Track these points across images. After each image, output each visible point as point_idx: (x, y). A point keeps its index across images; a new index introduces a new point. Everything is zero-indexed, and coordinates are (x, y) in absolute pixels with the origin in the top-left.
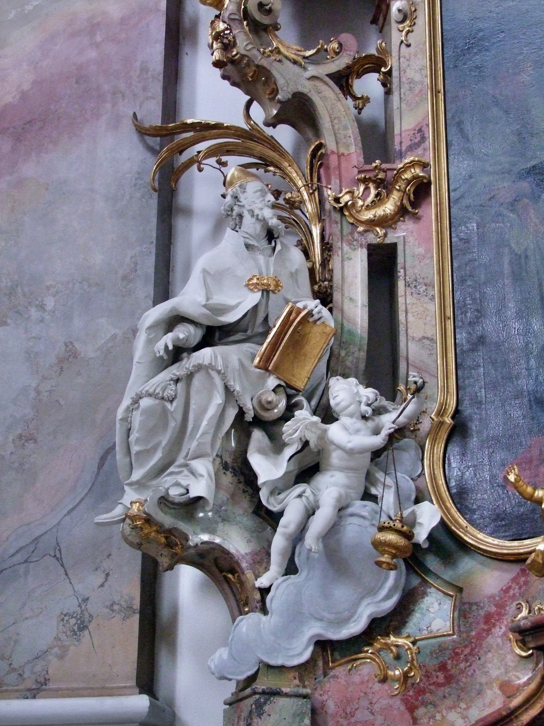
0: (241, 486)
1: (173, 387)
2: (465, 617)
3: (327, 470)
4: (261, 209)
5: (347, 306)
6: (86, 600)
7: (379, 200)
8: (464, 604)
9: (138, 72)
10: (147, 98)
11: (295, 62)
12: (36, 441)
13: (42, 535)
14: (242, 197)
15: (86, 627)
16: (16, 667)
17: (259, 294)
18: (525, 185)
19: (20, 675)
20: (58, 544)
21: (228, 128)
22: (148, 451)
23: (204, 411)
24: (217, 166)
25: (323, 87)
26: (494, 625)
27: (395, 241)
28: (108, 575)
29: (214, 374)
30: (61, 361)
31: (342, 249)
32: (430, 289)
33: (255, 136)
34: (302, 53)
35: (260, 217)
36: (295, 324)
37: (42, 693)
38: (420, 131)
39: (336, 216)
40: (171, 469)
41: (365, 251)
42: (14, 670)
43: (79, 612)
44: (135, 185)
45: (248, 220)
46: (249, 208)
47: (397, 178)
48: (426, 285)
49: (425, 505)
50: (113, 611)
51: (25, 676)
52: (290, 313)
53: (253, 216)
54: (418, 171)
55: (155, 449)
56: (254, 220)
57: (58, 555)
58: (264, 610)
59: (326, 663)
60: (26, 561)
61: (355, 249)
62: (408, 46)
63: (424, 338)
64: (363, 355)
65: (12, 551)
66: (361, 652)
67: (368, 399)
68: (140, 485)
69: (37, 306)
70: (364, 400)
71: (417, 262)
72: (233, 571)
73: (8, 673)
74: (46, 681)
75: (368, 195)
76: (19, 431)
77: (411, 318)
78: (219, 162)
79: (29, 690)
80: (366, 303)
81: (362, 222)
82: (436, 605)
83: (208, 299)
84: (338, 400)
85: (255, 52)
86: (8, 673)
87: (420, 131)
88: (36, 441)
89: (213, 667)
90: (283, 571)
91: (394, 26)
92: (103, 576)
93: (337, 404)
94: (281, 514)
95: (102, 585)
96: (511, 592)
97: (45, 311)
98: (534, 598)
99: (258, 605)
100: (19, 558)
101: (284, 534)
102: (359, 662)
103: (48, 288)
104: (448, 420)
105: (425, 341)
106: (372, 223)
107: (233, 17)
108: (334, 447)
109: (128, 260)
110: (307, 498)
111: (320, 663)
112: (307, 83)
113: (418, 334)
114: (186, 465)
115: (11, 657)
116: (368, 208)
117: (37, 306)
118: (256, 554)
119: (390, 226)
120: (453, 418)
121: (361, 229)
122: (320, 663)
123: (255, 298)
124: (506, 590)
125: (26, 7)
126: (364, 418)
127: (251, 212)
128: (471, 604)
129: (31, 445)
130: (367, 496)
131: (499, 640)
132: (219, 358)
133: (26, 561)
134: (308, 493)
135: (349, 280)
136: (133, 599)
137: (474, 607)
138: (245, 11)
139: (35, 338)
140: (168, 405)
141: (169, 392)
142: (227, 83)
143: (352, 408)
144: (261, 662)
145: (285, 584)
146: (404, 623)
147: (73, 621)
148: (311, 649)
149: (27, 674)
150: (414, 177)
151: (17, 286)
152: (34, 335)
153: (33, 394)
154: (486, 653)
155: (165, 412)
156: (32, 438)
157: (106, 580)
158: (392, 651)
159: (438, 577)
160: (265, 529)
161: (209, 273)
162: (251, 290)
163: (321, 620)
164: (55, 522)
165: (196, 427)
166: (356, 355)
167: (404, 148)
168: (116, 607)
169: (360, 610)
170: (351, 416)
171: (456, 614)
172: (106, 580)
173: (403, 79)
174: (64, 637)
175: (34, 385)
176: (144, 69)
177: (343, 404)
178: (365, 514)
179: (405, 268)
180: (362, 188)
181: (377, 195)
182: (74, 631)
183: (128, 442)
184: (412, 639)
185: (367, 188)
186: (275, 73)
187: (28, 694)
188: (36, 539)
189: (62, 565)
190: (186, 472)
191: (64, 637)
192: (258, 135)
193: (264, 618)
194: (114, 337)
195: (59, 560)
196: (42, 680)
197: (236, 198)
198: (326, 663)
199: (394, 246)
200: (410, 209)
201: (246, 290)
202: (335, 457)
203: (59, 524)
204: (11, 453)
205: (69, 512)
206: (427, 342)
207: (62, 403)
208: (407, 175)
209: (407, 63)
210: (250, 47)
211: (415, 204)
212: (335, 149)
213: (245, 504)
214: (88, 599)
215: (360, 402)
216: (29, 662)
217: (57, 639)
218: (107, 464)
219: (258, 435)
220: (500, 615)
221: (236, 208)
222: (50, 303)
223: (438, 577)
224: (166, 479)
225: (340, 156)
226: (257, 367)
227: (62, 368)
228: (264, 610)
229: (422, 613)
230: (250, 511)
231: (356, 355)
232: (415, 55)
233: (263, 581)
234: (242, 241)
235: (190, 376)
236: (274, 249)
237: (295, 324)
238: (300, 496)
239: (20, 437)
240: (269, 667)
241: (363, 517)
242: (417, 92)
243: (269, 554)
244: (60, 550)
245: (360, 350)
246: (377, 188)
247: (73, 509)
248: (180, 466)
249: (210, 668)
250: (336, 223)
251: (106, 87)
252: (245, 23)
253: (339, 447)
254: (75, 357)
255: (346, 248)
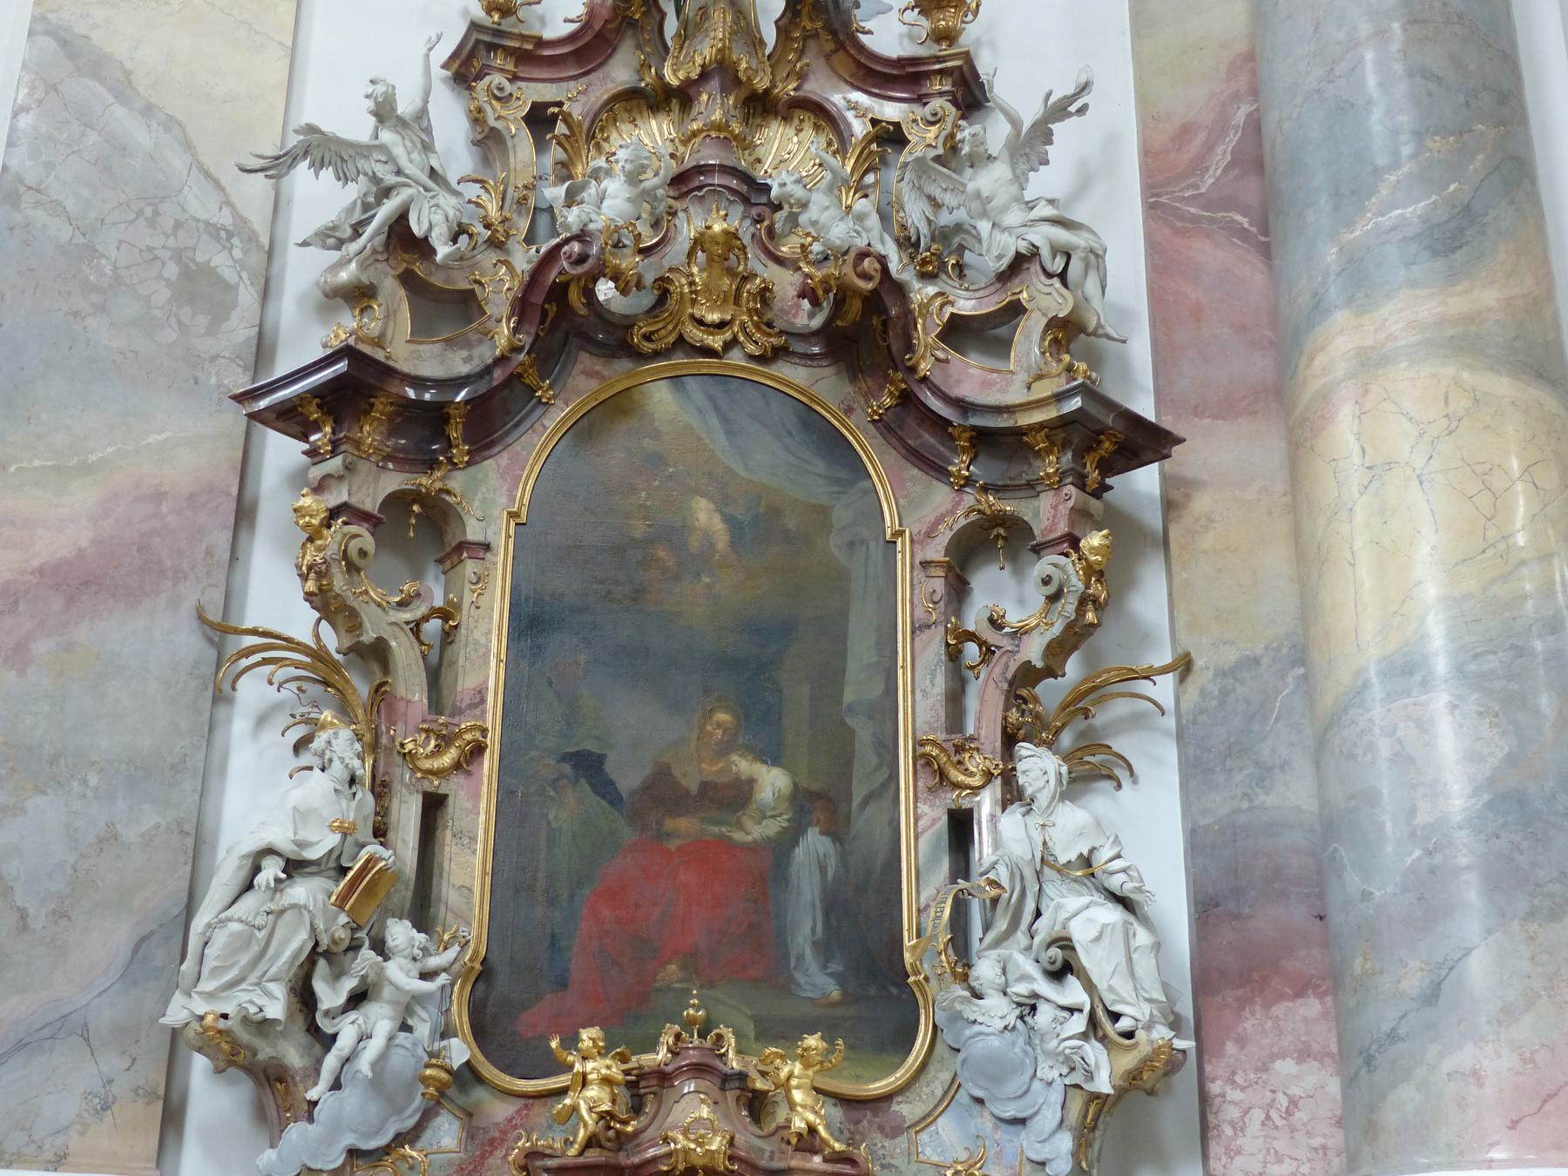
0: (299, 1006)
1: (265, 918)
2: (472, 1139)
3: (376, 1000)
4: (352, 759)
5: (399, 846)
6: (111, 1082)
7: (438, 751)
8: (473, 1127)
9: (203, 555)
10: (210, 585)
11: (379, 605)
12: (69, 919)
13: (71, 1013)
14: (334, 743)
15: (109, 1107)
16: (36, 1139)
17: (340, 835)
18: (567, 768)
19: (40, 1147)
20: (86, 1024)
21: (298, 643)
22: (225, 967)
23: (287, 941)
24: (297, 692)
25: (401, 634)
26: (496, 1148)
27: (447, 792)
28: (134, 1059)
29: (305, 913)
30: (101, 840)
31: (401, 791)
32: (473, 842)
33: (322, 657)
34: (386, 598)
35: (350, 766)
36: (373, 872)
37: (64, 1167)
38: (480, 692)
39: (399, 760)
40: (243, 986)
41: (420, 798)
42: (34, 1141)
43: (103, 1092)
44: (191, 674)
45: (337, 764)
46: (340, 755)
47: (459, 735)
48: (470, 838)
49: (455, 1042)
50: (137, 1095)
51: (44, 1148)
52: (368, 861)
53: (342, 763)
54: (478, 735)
55: (231, 966)
56: (342, 767)
57: (85, 1035)
58: (311, 1119)
59: (352, 1168)
60: (52, 1038)
61: (411, 793)
62: (478, 608)
63: (463, 886)
64: (409, 894)
65: (38, 1026)
66: (381, 1160)
67: (421, 943)
68: (210, 996)
69: (79, 780)
70: (417, 944)
71: (464, 816)
72: (281, 1080)
73: (28, 1144)
74: (65, 1156)
75: (429, 744)
76: (53, 906)
77: (453, 866)
78: (299, 689)
79: (50, 1162)
80: (417, 847)
81: (420, 770)
82: (447, 1125)
83: (295, 834)
84: (397, 942)
85: (350, 594)
86: (28, 1144)
87: (480, 692)
88: (69, 919)
89: (261, 1166)
90: (328, 1086)
91: (468, 586)
92: (131, 1060)
93: (396, 946)
94: (334, 1037)
95: (128, 1069)
96: (514, 1122)
97: (88, 786)
98: (532, 1130)
99: (306, 1115)
100: (46, 1033)
101: (337, 1056)
102: (379, 1169)
103: (93, 763)
104: (478, 967)
105: (464, 890)
106: (431, 772)
107: (334, 556)
108: (387, 982)
109: (177, 749)
110: (359, 1026)
111: (348, 1168)
112: (387, 627)
113: (459, 883)
114: (258, 984)
115: (31, 1128)
116: (427, 757)
117: (79, 780)
118: (307, 1069)
119: (444, 777)
120: (482, 964)
121: (419, 775)
122: (348, 1168)
123: (333, 840)
124: (510, 1121)
125: (90, 456)
126: (415, 959)
127: (342, 760)
128: (478, 1128)
129: (64, 922)
130: (405, 1027)
131: (499, 1161)
132: (311, 899)
133: (52, 1038)
134: (361, 1021)
135: (402, 822)
136: (158, 1085)
137: (481, 1131)
138: (345, 551)
139: (75, 813)
140: (256, 932)
141: (259, 921)
142: (307, 604)
143: (406, 952)
144: (304, 1165)
145: (331, 1099)
146: (417, 1137)
147: (96, 1101)
148: (344, 1156)
149: (47, 1147)
150: (474, 741)
151: (60, 756)
152: (74, 810)
153: (69, 871)
154: (487, 1171)
155: (251, 937)
156: (66, 915)
157: (133, 1063)
158: (408, 1162)
159: (452, 1101)
160: (313, 1046)
161: (298, 811)
162: (333, 831)
163: (355, 1132)
164: (84, 1002)
165: (277, 955)
166: (403, 893)
167: (464, 706)
168: (140, 1092)
169: (388, 1126)
170: (405, 957)
171: (464, 1134)
172: (133, 1063)
173: (470, 639)
174: (86, 1115)
175: (72, 860)
176: (209, 553)
177: (400, 947)
178: (409, 1046)
179: (453, 819)
180: (424, 736)
181: (435, 747)
182: (96, 1110)
183: (203, 954)
184: (425, 1153)
185: (427, 738)
186: (363, 615)
187: (50, 1166)
188: (64, 1017)
189: (89, 1046)
190: (259, 992)
191: (86, 1115)
192: (326, 657)
193: (310, 1127)
194: (158, 826)
195: (87, 1040)
196: (62, 1154)
197: (329, 742)
198: (352, 1168)
199: (445, 797)
200: (465, 765)
201: (327, 831)
202: (387, 992)
203: (88, 1004)
204: (44, 928)
205: (100, 994)
206: (465, 891)
207: (100, 884)
208: (468, 737)
209: (475, 624)
210: (345, 588)
211: (468, 763)
212: (404, 696)
213: (300, 1022)
214: (113, 1081)
215: (413, 946)
216: (49, 1135)
217: (79, 1116)
218: (140, 953)
219: (322, 964)
220: (503, 1140)
221: (327, 752)
222: (93, 779)
223: (452, 1101)
224: (240, 994)
225: (409, 702)
226: (333, 904)
227: (101, 849)
228: (311, 1119)
229: (434, 1131)
230: (304, 1028)
231: (403, 893)
232: (483, 618)
233: (312, 1094)
234: (331, 786)
235: (282, 912)
236: (354, 794)
237: (373, 872)
238: (353, 1023)
239: (54, 912)
240: (310, 1169)
241: (407, 1049)
242: (481, 654)
243: (318, 1072)
244: (88, 1030)
245: (407, 889)
246: (436, 740)
247: (104, 991)
248: (252, 984)
249: (258, 1166)
250: (399, 766)
251: (169, 564)
252: (343, 563)
253: (391, 983)
254: (116, 839)
255: (404, 791)
